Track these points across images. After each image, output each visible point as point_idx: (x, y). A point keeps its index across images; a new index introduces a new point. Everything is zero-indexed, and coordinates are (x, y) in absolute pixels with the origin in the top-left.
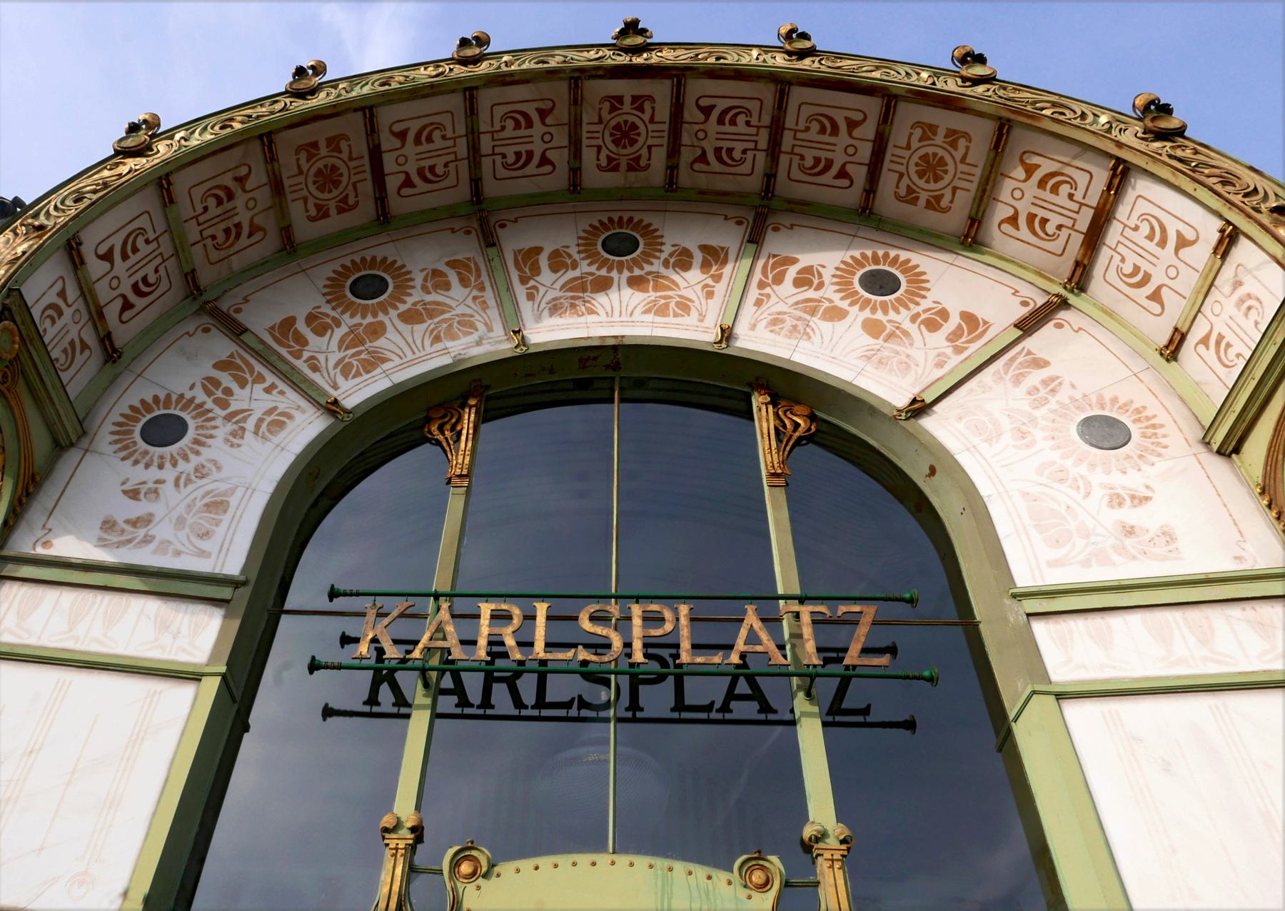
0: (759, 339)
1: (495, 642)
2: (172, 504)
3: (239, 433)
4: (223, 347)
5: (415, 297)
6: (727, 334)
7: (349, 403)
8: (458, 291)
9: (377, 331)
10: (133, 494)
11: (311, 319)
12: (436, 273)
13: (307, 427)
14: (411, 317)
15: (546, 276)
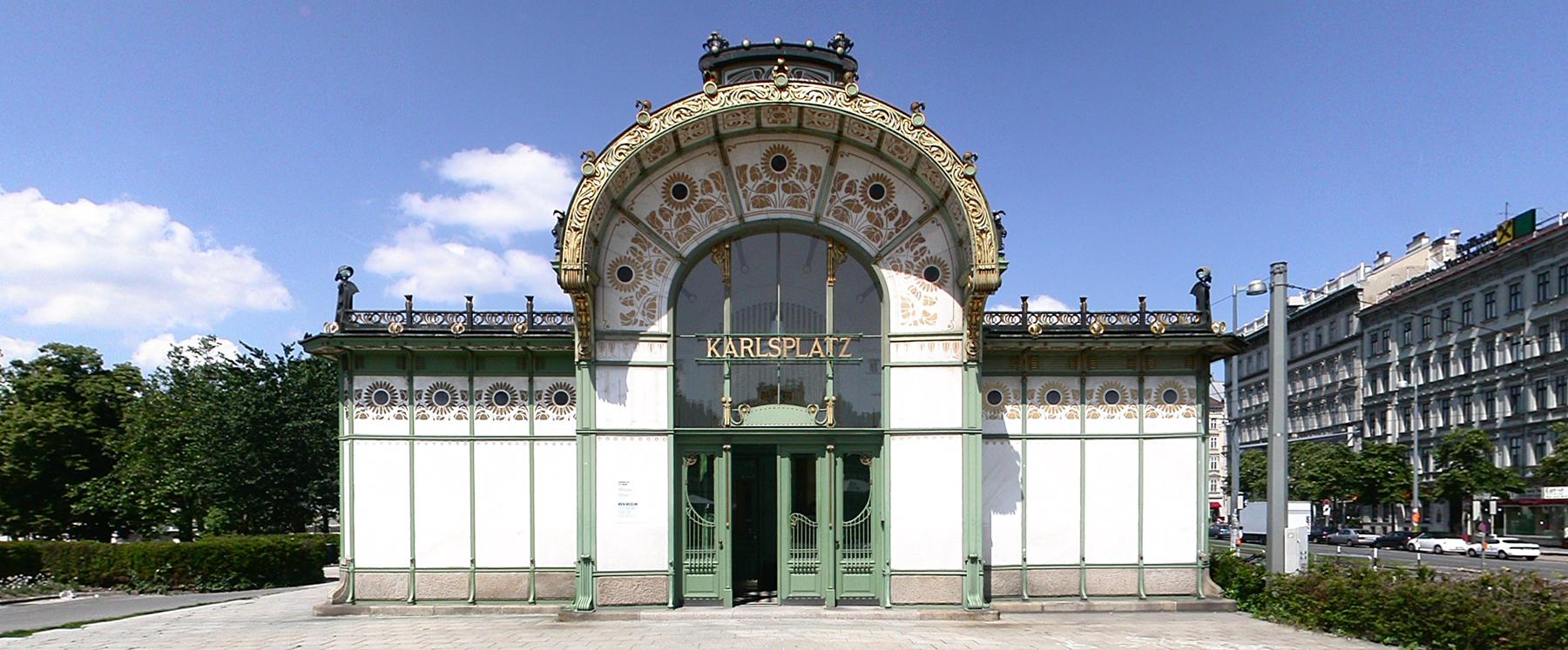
0: (830, 222)
1: (746, 352)
2: (638, 307)
3: (650, 272)
4: (631, 230)
5: (700, 196)
6: (817, 218)
7: (685, 254)
8: (716, 193)
9: (687, 216)
10: (624, 303)
11: (661, 211)
12: (706, 182)
13: (673, 268)
14: (699, 209)
15: (750, 184)
